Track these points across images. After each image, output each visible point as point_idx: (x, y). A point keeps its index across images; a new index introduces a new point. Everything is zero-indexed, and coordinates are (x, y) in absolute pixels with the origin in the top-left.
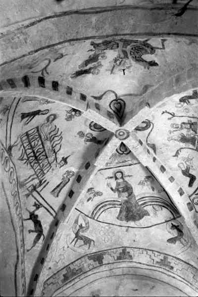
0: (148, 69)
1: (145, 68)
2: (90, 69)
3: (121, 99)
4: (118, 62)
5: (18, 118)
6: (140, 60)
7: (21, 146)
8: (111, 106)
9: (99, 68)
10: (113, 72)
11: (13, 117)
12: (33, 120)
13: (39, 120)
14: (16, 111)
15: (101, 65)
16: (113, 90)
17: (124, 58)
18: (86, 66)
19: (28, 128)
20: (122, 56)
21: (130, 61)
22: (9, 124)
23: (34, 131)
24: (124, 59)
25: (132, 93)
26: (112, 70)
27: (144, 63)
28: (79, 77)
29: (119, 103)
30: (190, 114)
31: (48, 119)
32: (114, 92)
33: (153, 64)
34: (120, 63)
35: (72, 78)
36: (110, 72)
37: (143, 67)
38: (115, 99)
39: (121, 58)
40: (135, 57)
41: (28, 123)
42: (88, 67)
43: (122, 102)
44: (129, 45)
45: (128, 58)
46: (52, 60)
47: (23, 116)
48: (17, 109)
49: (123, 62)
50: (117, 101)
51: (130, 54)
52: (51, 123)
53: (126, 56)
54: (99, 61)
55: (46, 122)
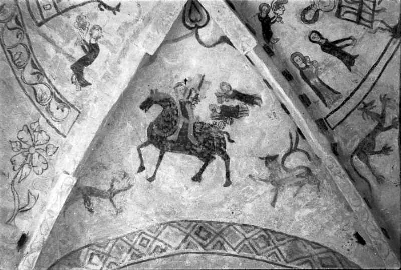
0: (152, 91)
1: (156, 90)
2: (233, 97)
3: (191, 28)
4: (194, 95)
5: (360, 67)
6: (163, 101)
7: (378, 11)
8: (206, 18)
9: (221, 92)
10: (200, 79)
11: (364, 80)
12: (340, 37)
13: (332, 29)
14: (356, 85)
15: (218, 97)
16: (202, 47)
17: (185, 103)
18: (237, 106)
19: (357, 30)
20: (188, 107)
21: (177, 98)
22: (374, 75)
23: (347, 12)
24: (186, 100)
25: (175, 44)
26: (202, 82)
27: (158, 100)
28: (250, 92)
29: (192, 21)
30: (74, 15)
31: (315, 18)
32: (201, 43)
33: (146, 106)
34: (191, 93)
35: (260, 99)
36: (206, 78)
37: (160, 91)
38: (200, 30)
39: (189, 102)
40: (171, 106)
41: (349, 38)
42: (235, 103)
43: (188, 23)
44: (182, 129)
45: (180, 102)
46: (280, 160)
47: (350, 61)
48: (353, 88)
49: (187, 95)
50: (196, 25)
51: (177, 111)
52: (313, 4)
53: (183, 105)
54: (220, 105)
55: (321, 12)
